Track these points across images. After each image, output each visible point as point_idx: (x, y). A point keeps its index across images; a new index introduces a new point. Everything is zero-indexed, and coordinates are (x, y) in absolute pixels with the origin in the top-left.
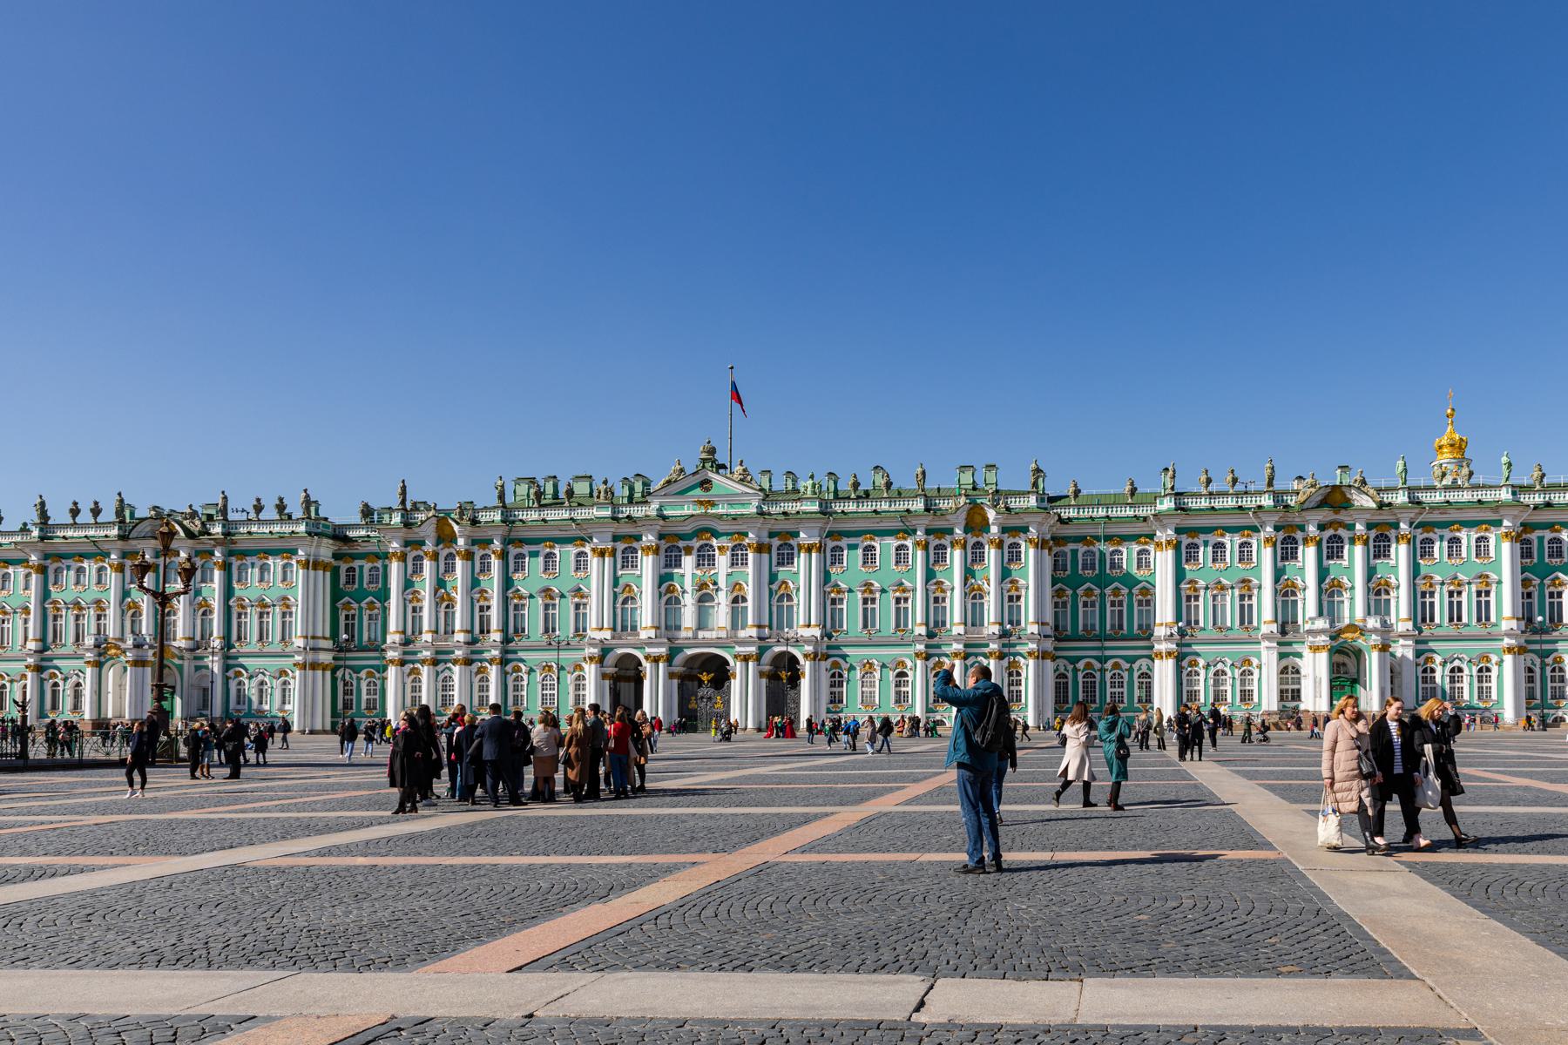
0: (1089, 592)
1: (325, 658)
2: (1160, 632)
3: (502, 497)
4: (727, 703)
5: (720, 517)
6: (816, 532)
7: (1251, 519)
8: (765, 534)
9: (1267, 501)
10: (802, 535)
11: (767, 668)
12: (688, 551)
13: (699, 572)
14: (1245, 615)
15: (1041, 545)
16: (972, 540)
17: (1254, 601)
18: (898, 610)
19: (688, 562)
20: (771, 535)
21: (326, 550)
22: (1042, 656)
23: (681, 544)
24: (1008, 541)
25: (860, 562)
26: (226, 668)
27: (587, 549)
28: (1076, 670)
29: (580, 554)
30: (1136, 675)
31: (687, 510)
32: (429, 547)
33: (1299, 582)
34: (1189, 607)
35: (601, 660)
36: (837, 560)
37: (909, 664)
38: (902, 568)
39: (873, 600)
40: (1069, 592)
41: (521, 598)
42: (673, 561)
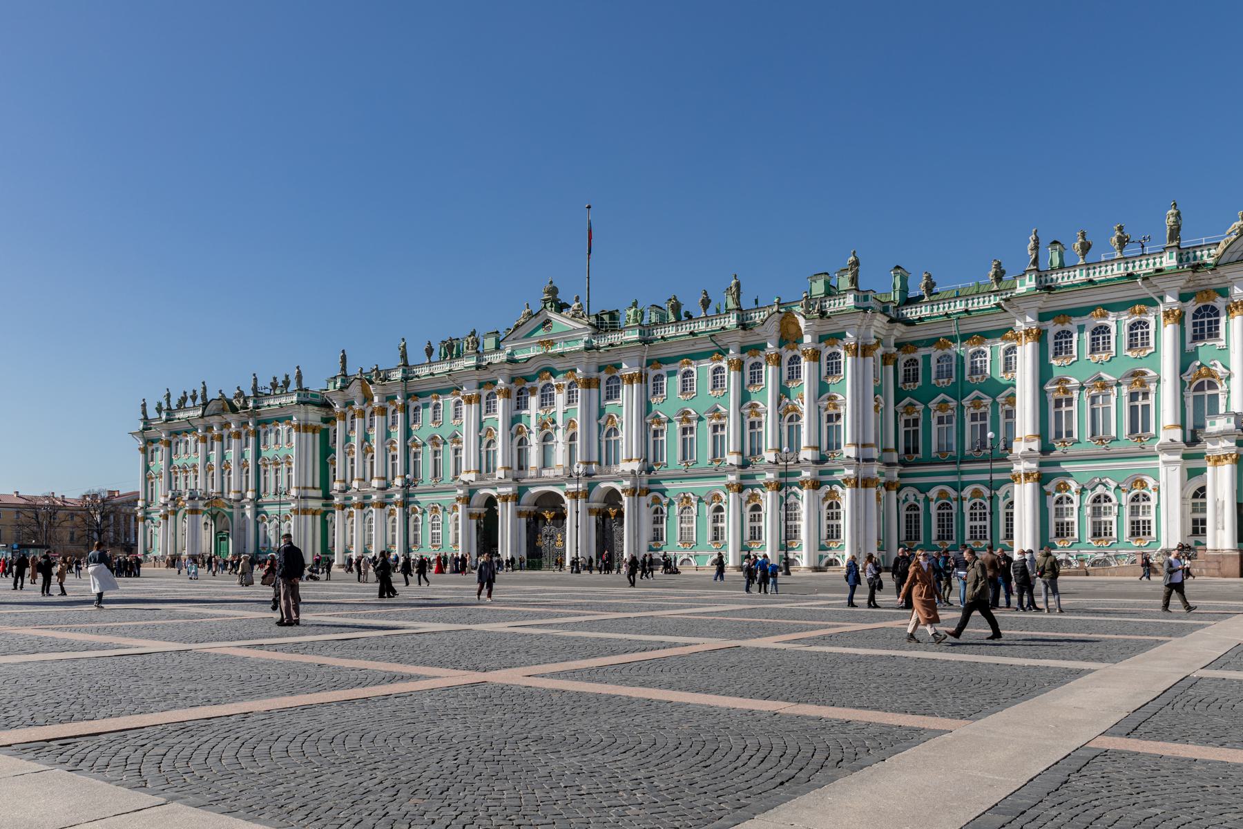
0: (943, 405)
1: (316, 505)
2: (1019, 448)
3: (404, 356)
4: (564, 541)
5: (553, 356)
6: (637, 361)
8: (593, 368)
9: (1169, 261)
10: (624, 366)
11: (596, 505)
12: (533, 391)
13: (541, 412)
14: (1139, 420)
17: (1151, 400)
18: (715, 438)
19: (533, 401)
21: (314, 416)
22: (862, 483)
23: (528, 385)
24: (826, 351)
25: (679, 389)
26: (257, 514)
28: (928, 500)
29: (458, 403)
31: (534, 351)
32: (357, 407)
33: (1219, 369)
34: (1058, 415)
35: (467, 500)
36: (658, 389)
37: (724, 497)
38: (719, 392)
39: (692, 429)
40: (920, 407)
41: (417, 446)
42: (522, 404)
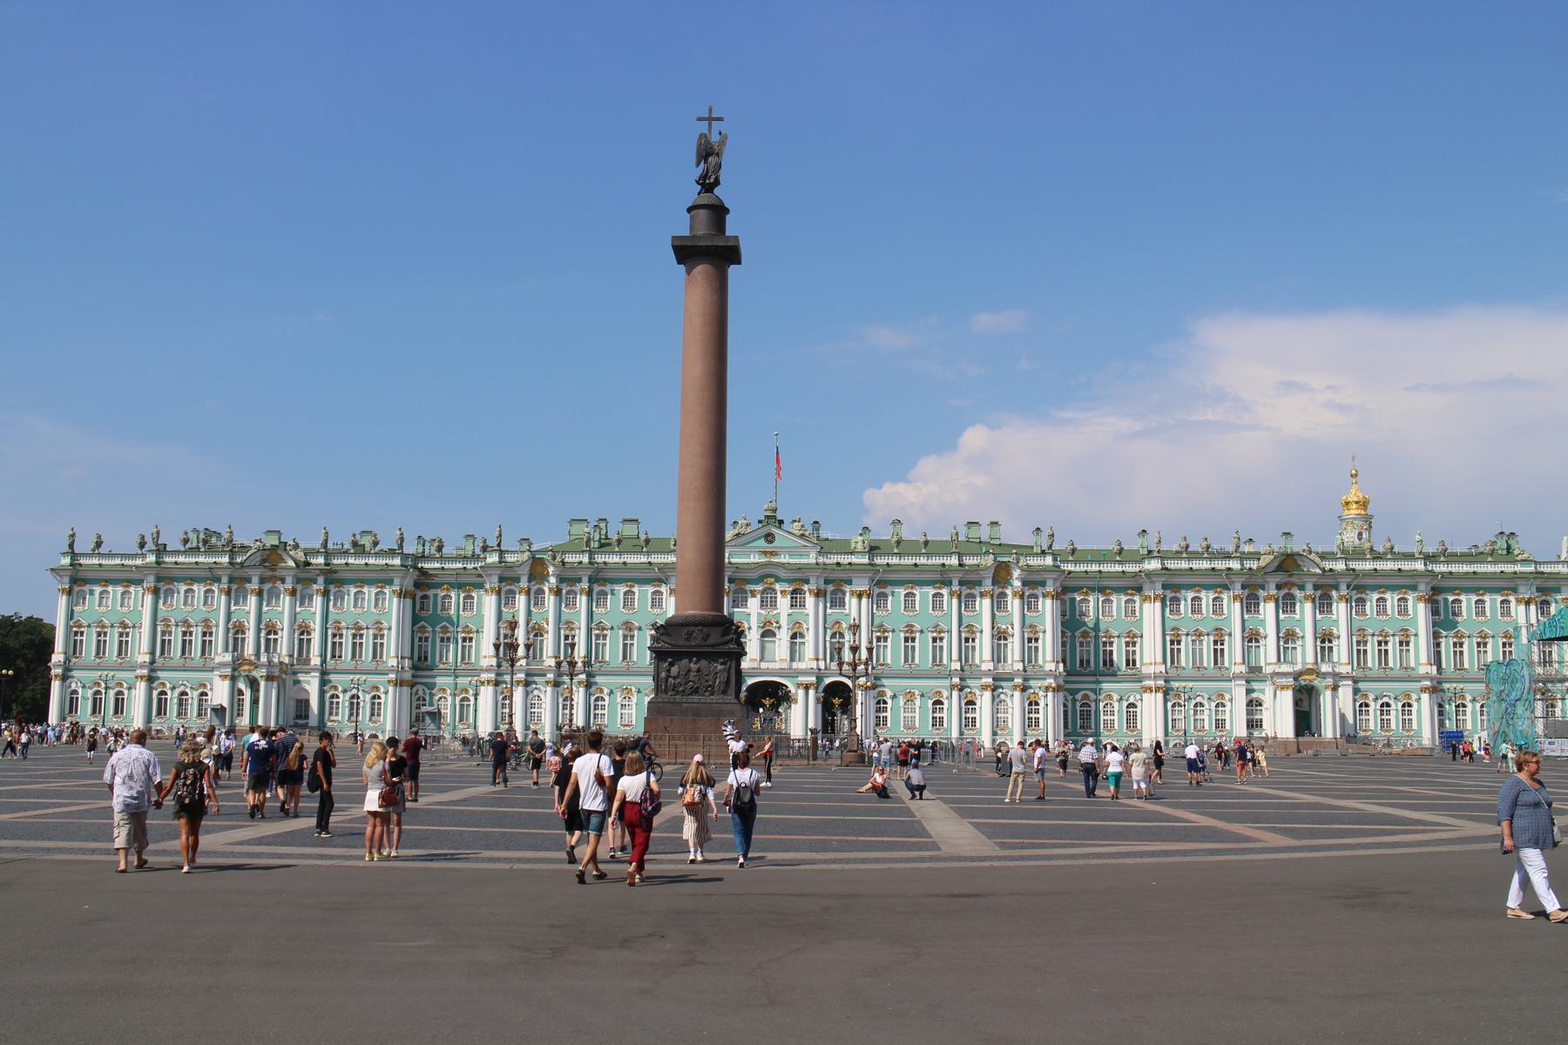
5: (782, 565)
7: (1224, 580)
15: (1056, 596)
16: (998, 591)
18: (934, 648)
20: (827, 582)
23: (749, 587)
27: (663, 589)
30: (1125, 704)
31: (755, 559)
32: (524, 583)
37: (945, 694)
39: (913, 640)
